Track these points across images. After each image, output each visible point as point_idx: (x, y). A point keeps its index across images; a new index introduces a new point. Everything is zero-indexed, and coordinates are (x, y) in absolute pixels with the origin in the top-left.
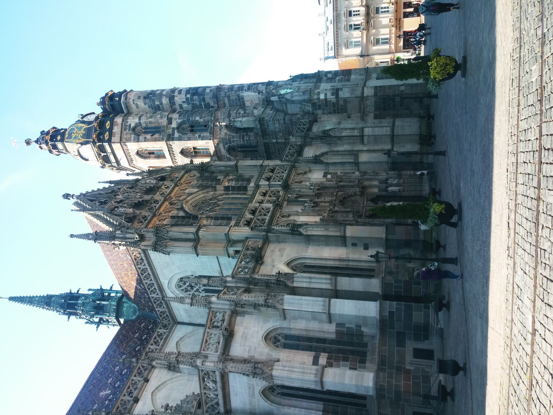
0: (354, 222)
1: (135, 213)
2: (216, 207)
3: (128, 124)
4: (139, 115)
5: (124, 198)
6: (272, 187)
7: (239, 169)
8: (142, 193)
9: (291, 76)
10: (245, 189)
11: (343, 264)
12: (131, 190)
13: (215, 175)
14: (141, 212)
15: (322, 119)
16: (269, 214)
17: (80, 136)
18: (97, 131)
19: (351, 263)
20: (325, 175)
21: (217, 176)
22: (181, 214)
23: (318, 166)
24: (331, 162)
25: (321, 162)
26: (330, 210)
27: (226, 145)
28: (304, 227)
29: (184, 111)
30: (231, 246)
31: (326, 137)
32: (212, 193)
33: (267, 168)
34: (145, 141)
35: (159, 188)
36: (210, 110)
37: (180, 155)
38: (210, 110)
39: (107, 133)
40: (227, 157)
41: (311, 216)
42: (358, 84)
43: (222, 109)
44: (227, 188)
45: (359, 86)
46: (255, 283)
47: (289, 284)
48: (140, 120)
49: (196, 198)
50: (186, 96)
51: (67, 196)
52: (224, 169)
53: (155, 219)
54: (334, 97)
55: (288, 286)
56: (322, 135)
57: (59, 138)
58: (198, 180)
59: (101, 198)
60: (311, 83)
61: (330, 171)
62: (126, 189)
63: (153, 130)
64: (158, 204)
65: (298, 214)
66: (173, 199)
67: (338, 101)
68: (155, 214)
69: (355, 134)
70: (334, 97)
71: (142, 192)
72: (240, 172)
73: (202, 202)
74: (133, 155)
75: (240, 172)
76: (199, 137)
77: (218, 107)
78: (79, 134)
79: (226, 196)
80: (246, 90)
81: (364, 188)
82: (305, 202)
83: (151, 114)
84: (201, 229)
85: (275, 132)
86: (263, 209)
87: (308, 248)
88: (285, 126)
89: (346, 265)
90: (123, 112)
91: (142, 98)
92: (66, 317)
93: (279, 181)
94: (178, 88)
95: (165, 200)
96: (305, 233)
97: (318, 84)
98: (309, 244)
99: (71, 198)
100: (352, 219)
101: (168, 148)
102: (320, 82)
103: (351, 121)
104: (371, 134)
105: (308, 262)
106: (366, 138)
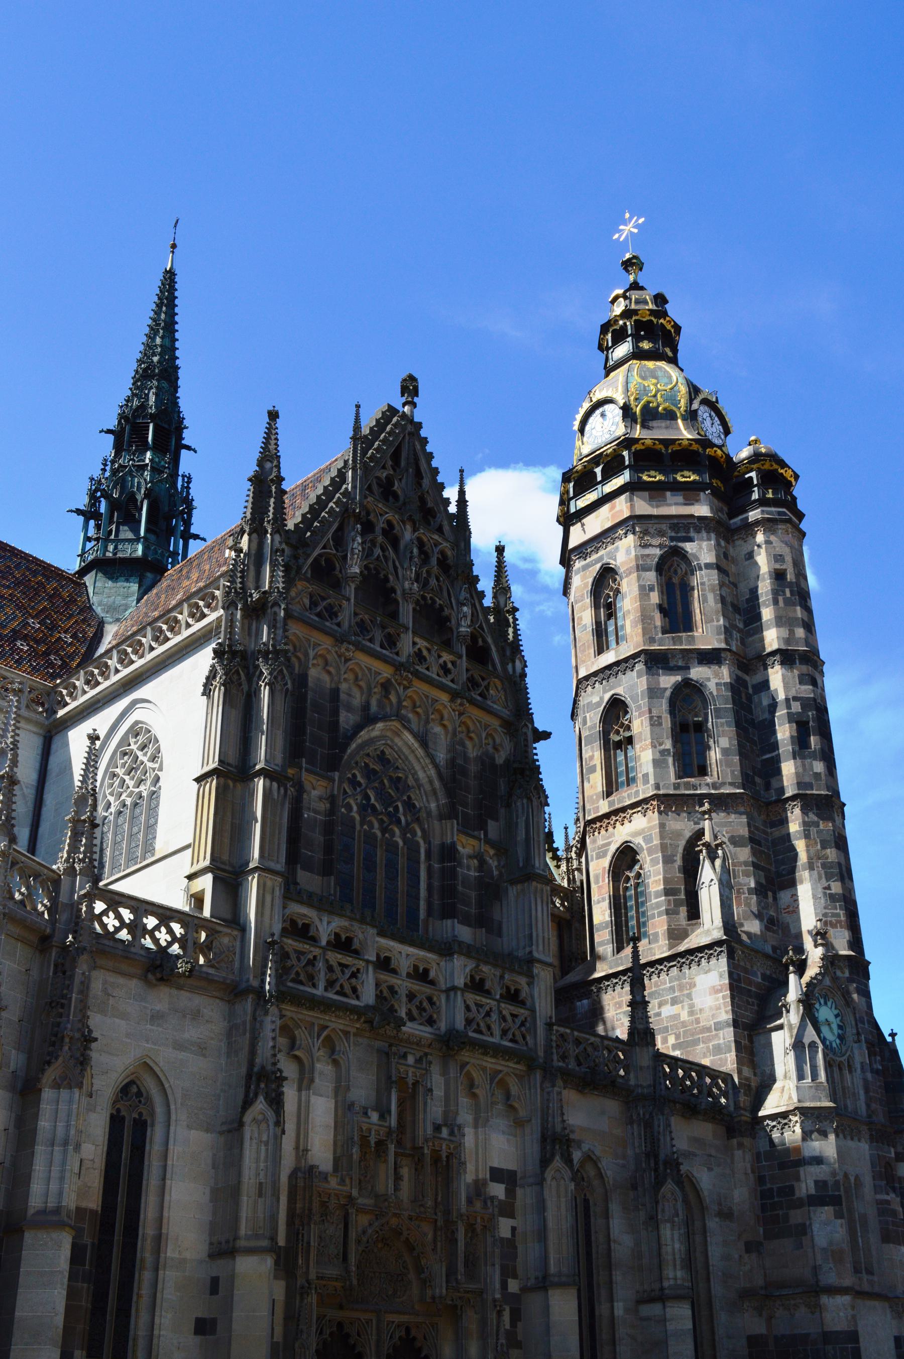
0: (300, 1281)
2: (381, 822)
3: (692, 534)
4: (724, 564)
5: (406, 546)
6: (448, 998)
7: (519, 887)
8: (424, 598)
9: (893, 1035)
10: (448, 912)
11: (145, 1251)
12: (434, 561)
14: (348, 600)
15: (738, 1153)
16: (331, 995)
17: (649, 402)
18: (667, 448)
19: (147, 1275)
20: (497, 1175)
21: (497, 820)
22: (346, 719)
23: (536, 1147)
24: (546, 1193)
25: (545, 1162)
26: (350, 1197)
27: (644, 839)
28: (270, 1114)
29: (749, 698)
30: (215, 880)
31: (656, 1170)
32: (433, 805)
33: (523, 981)
34: (642, 588)
35: (447, 645)
36: (758, 780)
37: (607, 697)
38: (758, 780)
39: (660, 477)
40: (609, 844)
41: (335, 1136)
42: (870, 1272)
43: (763, 817)
44: (449, 853)
45: (865, 1277)
46: (63, 965)
47: (51, 1074)
48: (708, 566)
49: (411, 758)
50: (795, 699)
51: (410, 387)
52: (519, 839)
53: (326, 642)
54: (812, 1191)
55: (43, 1071)
56: (662, 1156)
57: (646, 345)
59: (404, 481)
60: (868, 1106)
61: (519, 1192)
62: (436, 550)
63: (680, 609)
64: (382, 646)
65: (340, 1089)
67: (800, 1204)
68: (342, 643)
69: (669, 1272)
70: (812, 1191)
71: (428, 596)
72: (513, 891)
73: (399, 778)
74: (601, 558)
75: (513, 891)
76: (663, 753)
77: (768, 804)
78: (655, 396)
79: (422, 851)
80: (829, 888)
81: (454, 1312)
82: (384, 1114)
83: (729, 599)
84: (275, 785)
85: (689, 996)
86: (354, 975)
87: (207, 1131)
88: (708, 1029)
89: (143, 1260)
90: (731, 516)
91: (778, 566)
92: (112, 424)
93: (469, 1022)
94: (822, 673)
96: (248, 1118)
97: (864, 1128)
98: (221, 1133)
99: (404, 400)
100: (312, 1276)
101: (626, 660)
102: (872, 1139)
103: (736, 1256)
104: (670, 1327)
105: (156, 1134)
106: (655, 1309)
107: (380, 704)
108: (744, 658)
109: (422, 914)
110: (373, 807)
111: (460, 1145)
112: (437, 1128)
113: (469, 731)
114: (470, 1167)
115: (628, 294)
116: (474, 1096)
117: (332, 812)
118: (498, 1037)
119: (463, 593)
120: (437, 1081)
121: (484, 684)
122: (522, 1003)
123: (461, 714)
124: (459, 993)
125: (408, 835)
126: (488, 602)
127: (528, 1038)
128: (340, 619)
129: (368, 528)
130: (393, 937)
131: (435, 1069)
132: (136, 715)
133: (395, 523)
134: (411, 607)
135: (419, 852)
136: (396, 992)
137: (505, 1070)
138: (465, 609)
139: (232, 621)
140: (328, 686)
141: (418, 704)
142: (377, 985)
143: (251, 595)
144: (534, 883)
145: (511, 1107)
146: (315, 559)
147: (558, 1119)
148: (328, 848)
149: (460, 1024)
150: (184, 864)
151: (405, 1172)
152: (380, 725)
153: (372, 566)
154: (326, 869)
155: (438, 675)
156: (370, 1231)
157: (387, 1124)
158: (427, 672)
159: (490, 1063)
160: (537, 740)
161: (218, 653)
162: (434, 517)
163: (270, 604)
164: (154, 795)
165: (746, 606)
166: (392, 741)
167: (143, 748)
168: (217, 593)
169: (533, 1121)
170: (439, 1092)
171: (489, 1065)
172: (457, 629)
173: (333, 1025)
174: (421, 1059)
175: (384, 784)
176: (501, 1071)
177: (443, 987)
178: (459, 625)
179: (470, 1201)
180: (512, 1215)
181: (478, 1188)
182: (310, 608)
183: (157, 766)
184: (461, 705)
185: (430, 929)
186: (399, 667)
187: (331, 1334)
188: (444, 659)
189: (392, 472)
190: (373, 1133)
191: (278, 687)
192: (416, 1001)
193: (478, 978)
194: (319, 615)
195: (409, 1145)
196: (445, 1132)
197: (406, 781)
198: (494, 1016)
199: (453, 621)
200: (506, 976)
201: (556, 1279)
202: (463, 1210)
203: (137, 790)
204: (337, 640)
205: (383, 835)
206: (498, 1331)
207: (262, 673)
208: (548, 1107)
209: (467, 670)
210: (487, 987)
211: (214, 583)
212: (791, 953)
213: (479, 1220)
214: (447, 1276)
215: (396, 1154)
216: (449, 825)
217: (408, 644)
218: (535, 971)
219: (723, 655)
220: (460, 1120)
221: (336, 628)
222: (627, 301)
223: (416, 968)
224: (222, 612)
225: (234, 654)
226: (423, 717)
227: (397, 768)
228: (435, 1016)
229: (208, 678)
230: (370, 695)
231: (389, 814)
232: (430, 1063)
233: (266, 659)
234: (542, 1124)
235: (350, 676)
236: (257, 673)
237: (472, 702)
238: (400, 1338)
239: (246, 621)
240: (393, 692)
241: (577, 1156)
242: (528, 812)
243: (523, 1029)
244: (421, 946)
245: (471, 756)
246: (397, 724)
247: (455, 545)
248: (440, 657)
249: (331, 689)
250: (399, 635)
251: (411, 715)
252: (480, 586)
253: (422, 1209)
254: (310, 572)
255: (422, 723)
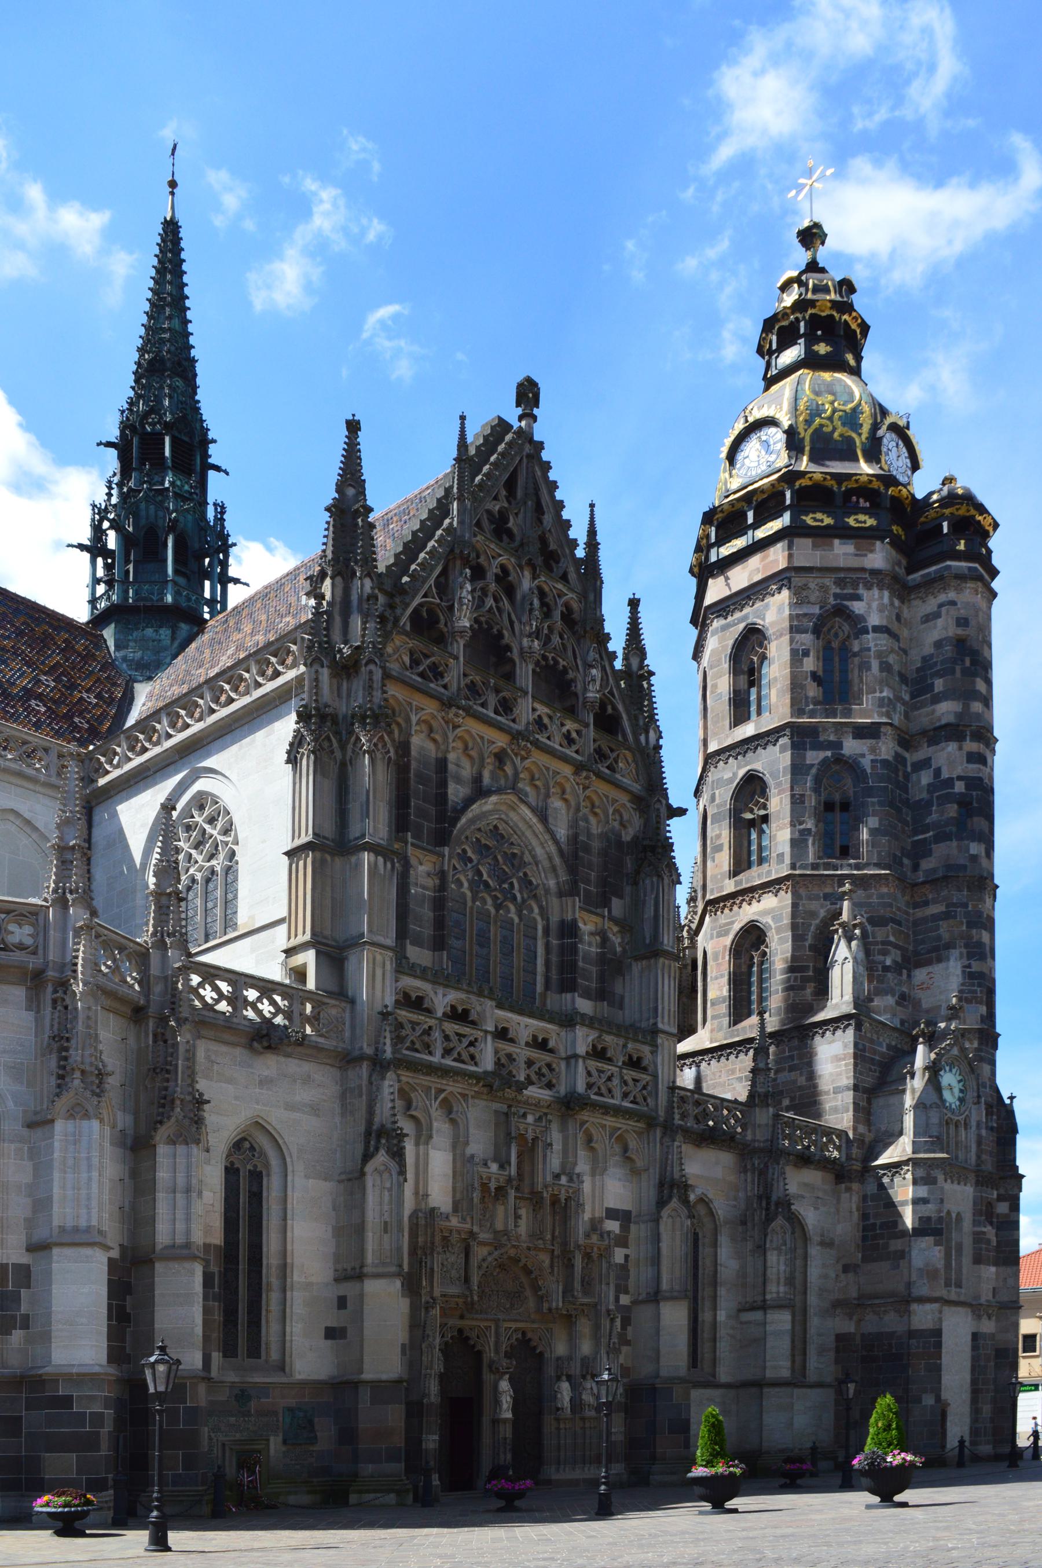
1: (453, 637)
13: (628, 889)
49: (528, 833)
58: (603, 836)
66: (518, 761)
73: (514, 855)
95: (516, 736)
107: (493, 776)
108: (906, 733)
109: (539, 988)
110: (486, 885)
111: (578, 1191)
112: (557, 1177)
113: (593, 806)
114: (588, 1208)
115: (804, 278)
116: (592, 1149)
117: (442, 887)
118: (619, 1098)
119: (591, 653)
120: (556, 1137)
121: (613, 755)
122: (645, 1069)
123: (585, 788)
124: (580, 1061)
125: (525, 912)
126: (618, 664)
127: (649, 1100)
128: (446, 680)
129: (478, 573)
130: (512, 1009)
131: (555, 1127)
132: (202, 785)
133: (510, 567)
134: (531, 667)
135: (536, 929)
136: (514, 1060)
137: (625, 1127)
139: (317, 680)
140: (434, 755)
141: (537, 776)
142: (496, 1052)
143: (340, 651)
144: (661, 960)
145: (629, 1158)
146: (416, 611)
147: (676, 1169)
148: (439, 923)
149: (581, 1087)
150: (280, 937)
151: (523, 1212)
152: (494, 799)
153: (483, 619)
154: (438, 944)
156: (490, 1259)
157: (506, 1173)
158: (548, 742)
159: (610, 1121)
160: (670, 817)
161: (303, 717)
162: (558, 562)
163: (364, 662)
164: (230, 871)
165: (915, 675)
166: (507, 815)
167: (212, 821)
168: (294, 648)
169: (651, 1170)
170: (557, 1146)
171: (608, 1123)
172: (584, 694)
173: (449, 1089)
174: (540, 1118)
175: (497, 860)
176: (620, 1129)
177: (563, 1055)
178: (585, 690)
179: (587, 1236)
180: (625, 1245)
181: (595, 1226)
183: (230, 839)
184: (587, 778)
185: (548, 1001)
186: (516, 736)
187: (452, 1338)
188: (567, 727)
190: (493, 1180)
191: (379, 755)
192: (535, 1067)
193: (599, 1047)
194: (421, 675)
195: (527, 1190)
196: (564, 1180)
197: (522, 858)
198: (616, 1081)
199: (579, 686)
200: (629, 1046)
201: (667, 1294)
202: (581, 1242)
203: (208, 864)
204: (443, 704)
205: (497, 911)
206: (610, 1333)
207: (358, 739)
208: (667, 1159)
209: (594, 741)
210: (609, 1055)
211: (289, 636)
212: (922, 1026)
213: (595, 1249)
214: (563, 1293)
215: (516, 1197)
216: (569, 904)
217: (527, 710)
218: (659, 1041)
219: (882, 730)
220: (578, 1170)
221: (442, 690)
222: (803, 290)
223: (535, 1038)
224: (302, 669)
225: (323, 717)
226: (542, 791)
227: (512, 844)
228: (554, 1081)
229: (291, 745)
230: (482, 766)
231: (503, 891)
232: (550, 1121)
233: (363, 724)
234: (661, 1175)
235: (459, 744)
236: (353, 739)
237: (599, 775)
238: (517, 1339)
239: (335, 681)
240: (508, 763)
241: (692, 1197)
242: (658, 890)
243: (644, 1092)
244: (541, 1017)
245: (595, 832)
246: (514, 798)
247: (583, 596)
248: (563, 725)
249: (437, 759)
250: (515, 700)
251: (528, 789)
252: (612, 646)
253: (541, 1242)
254: (408, 624)
255: (541, 797)
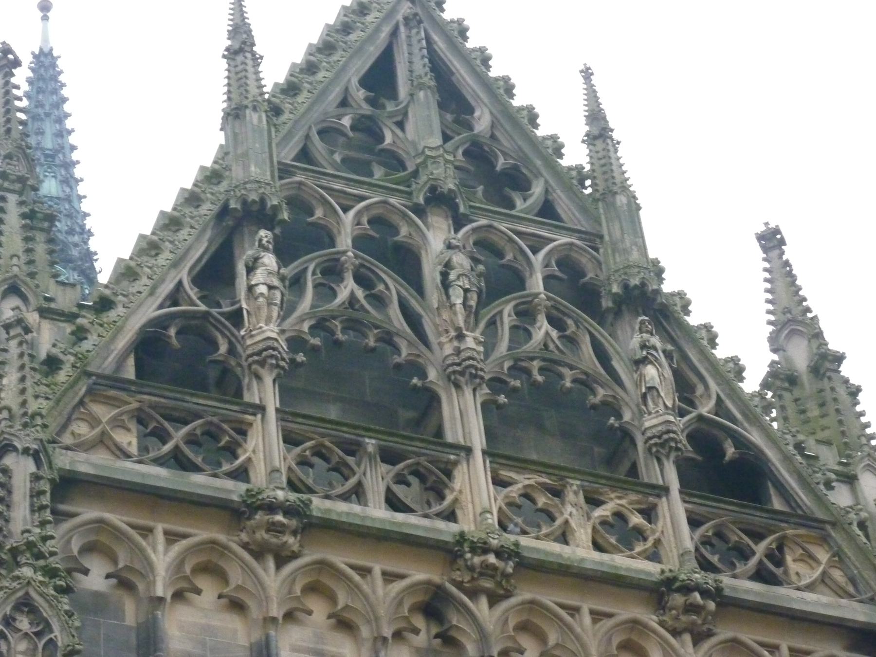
14: (261, 409)
138: (650, 371)
155: (597, 547)
182: (144, 449)
189: (367, 109)
